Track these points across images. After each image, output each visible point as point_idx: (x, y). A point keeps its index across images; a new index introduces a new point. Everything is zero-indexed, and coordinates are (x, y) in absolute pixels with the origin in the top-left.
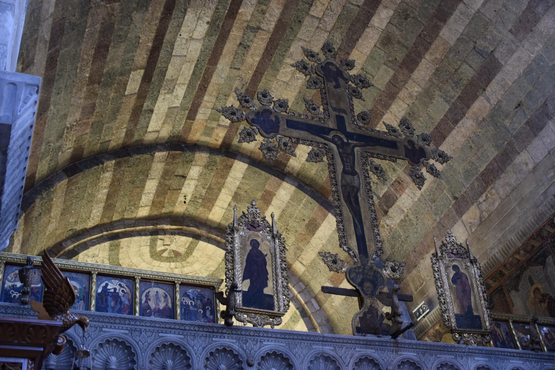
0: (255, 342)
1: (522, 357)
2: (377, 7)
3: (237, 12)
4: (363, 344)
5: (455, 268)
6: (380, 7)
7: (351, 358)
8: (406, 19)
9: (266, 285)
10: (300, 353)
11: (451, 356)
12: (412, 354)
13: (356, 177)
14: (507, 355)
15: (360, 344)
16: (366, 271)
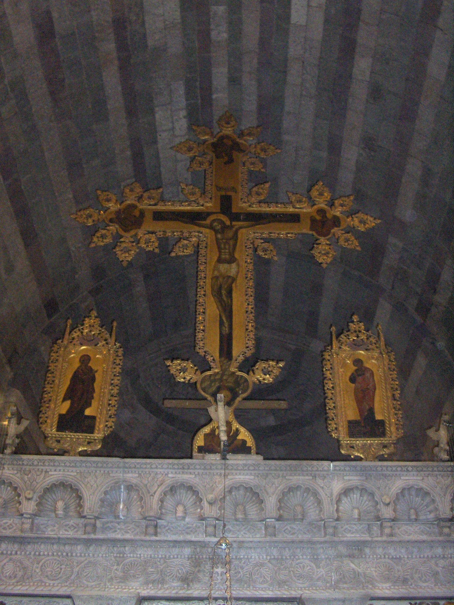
0: (38, 473)
1: (422, 471)
2: (353, 58)
3: (211, 99)
4: (178, 469)
5: (358, 362)
6: (357, 57)
7: (159, 486)
8: (387, 63)
9: (89, 405)
10: (92, 482)
11: (307, 478)
12: (247, 477)
13: (234, 265)
14: (397, 471)
15: (174, 469)
16: (224, 378)
